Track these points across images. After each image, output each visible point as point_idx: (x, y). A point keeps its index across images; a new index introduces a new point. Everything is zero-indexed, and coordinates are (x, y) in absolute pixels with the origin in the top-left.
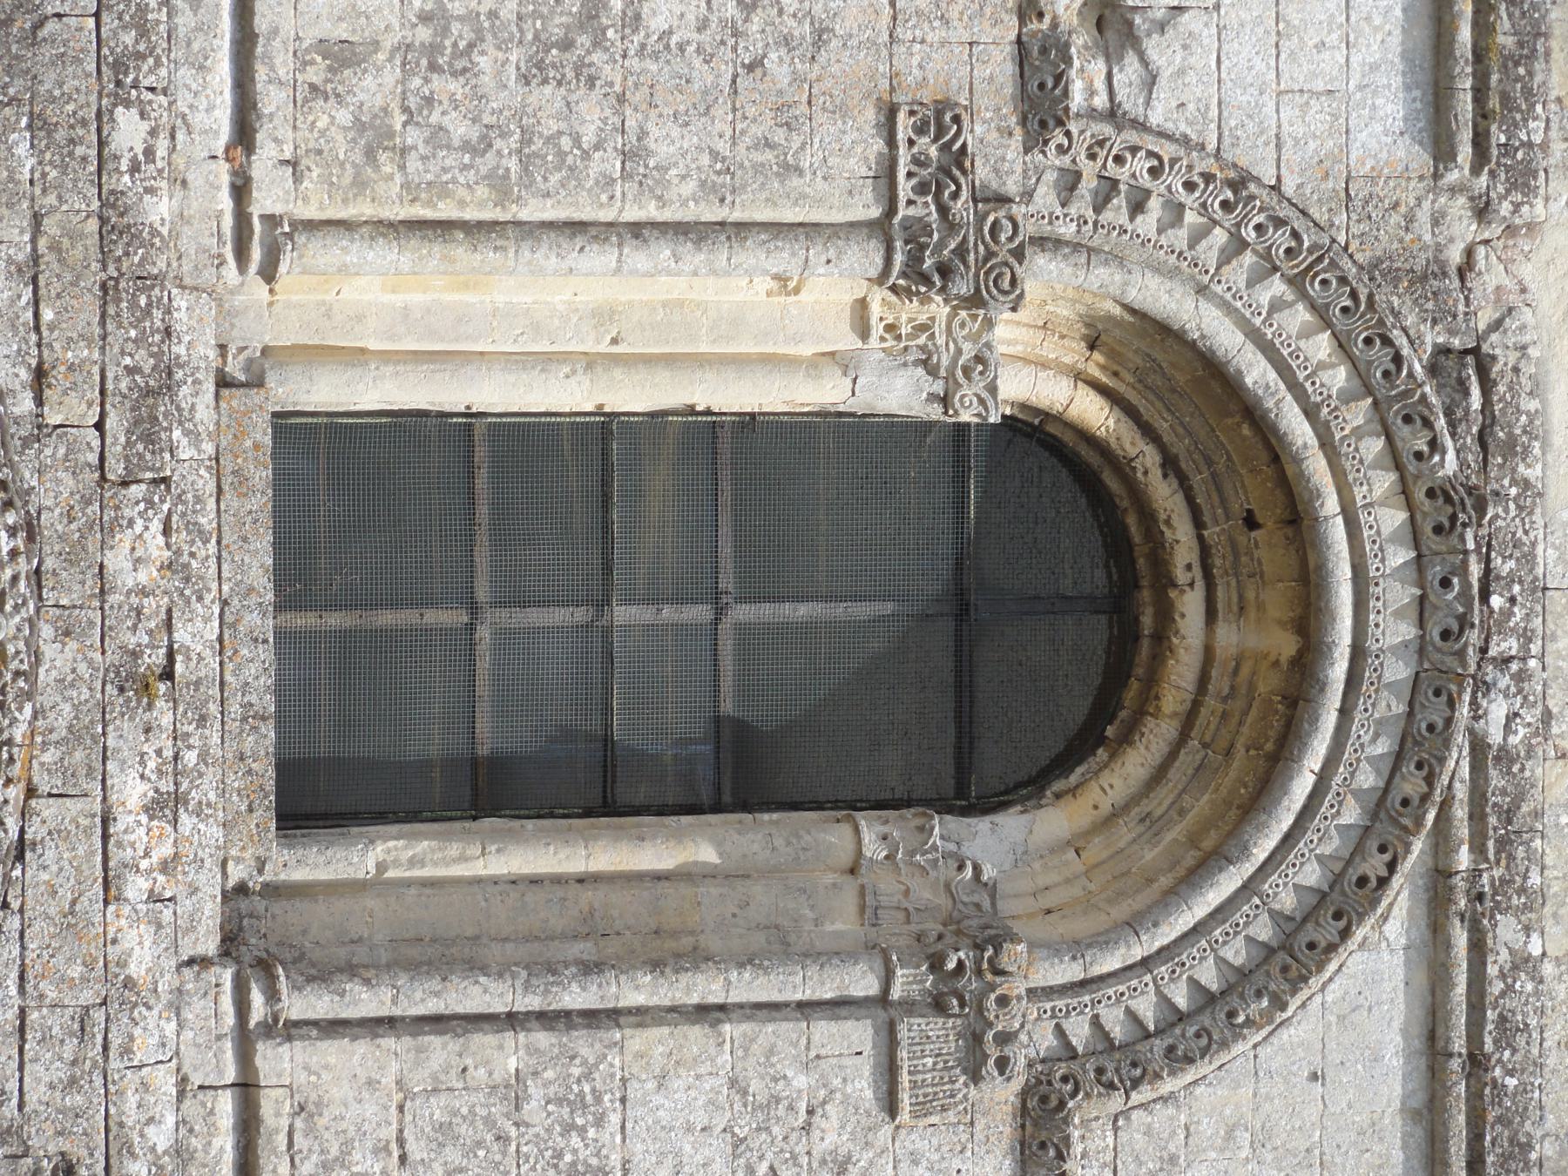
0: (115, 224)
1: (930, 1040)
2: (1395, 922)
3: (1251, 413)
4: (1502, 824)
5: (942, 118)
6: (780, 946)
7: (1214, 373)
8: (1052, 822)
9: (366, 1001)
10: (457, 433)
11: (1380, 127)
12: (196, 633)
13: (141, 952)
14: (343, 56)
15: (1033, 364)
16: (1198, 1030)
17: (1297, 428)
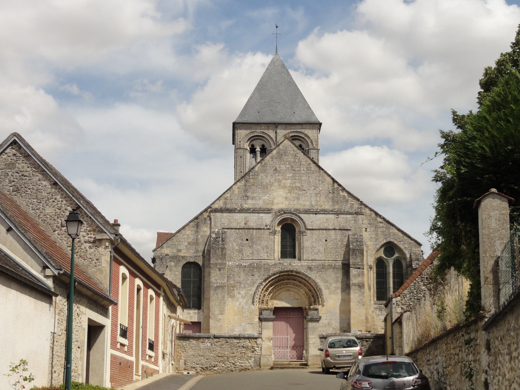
0: (274, 265)
1: (304, 234)
2: (300, 215)
3: (281, 220)
4: (297, 210)
5: (270, 233)
6: (300, 239)
7: (280, 222)
10: (281, 251)
11: (270, 215)
12: (288, 262)
13: (300, 264)
15: (279, 229)
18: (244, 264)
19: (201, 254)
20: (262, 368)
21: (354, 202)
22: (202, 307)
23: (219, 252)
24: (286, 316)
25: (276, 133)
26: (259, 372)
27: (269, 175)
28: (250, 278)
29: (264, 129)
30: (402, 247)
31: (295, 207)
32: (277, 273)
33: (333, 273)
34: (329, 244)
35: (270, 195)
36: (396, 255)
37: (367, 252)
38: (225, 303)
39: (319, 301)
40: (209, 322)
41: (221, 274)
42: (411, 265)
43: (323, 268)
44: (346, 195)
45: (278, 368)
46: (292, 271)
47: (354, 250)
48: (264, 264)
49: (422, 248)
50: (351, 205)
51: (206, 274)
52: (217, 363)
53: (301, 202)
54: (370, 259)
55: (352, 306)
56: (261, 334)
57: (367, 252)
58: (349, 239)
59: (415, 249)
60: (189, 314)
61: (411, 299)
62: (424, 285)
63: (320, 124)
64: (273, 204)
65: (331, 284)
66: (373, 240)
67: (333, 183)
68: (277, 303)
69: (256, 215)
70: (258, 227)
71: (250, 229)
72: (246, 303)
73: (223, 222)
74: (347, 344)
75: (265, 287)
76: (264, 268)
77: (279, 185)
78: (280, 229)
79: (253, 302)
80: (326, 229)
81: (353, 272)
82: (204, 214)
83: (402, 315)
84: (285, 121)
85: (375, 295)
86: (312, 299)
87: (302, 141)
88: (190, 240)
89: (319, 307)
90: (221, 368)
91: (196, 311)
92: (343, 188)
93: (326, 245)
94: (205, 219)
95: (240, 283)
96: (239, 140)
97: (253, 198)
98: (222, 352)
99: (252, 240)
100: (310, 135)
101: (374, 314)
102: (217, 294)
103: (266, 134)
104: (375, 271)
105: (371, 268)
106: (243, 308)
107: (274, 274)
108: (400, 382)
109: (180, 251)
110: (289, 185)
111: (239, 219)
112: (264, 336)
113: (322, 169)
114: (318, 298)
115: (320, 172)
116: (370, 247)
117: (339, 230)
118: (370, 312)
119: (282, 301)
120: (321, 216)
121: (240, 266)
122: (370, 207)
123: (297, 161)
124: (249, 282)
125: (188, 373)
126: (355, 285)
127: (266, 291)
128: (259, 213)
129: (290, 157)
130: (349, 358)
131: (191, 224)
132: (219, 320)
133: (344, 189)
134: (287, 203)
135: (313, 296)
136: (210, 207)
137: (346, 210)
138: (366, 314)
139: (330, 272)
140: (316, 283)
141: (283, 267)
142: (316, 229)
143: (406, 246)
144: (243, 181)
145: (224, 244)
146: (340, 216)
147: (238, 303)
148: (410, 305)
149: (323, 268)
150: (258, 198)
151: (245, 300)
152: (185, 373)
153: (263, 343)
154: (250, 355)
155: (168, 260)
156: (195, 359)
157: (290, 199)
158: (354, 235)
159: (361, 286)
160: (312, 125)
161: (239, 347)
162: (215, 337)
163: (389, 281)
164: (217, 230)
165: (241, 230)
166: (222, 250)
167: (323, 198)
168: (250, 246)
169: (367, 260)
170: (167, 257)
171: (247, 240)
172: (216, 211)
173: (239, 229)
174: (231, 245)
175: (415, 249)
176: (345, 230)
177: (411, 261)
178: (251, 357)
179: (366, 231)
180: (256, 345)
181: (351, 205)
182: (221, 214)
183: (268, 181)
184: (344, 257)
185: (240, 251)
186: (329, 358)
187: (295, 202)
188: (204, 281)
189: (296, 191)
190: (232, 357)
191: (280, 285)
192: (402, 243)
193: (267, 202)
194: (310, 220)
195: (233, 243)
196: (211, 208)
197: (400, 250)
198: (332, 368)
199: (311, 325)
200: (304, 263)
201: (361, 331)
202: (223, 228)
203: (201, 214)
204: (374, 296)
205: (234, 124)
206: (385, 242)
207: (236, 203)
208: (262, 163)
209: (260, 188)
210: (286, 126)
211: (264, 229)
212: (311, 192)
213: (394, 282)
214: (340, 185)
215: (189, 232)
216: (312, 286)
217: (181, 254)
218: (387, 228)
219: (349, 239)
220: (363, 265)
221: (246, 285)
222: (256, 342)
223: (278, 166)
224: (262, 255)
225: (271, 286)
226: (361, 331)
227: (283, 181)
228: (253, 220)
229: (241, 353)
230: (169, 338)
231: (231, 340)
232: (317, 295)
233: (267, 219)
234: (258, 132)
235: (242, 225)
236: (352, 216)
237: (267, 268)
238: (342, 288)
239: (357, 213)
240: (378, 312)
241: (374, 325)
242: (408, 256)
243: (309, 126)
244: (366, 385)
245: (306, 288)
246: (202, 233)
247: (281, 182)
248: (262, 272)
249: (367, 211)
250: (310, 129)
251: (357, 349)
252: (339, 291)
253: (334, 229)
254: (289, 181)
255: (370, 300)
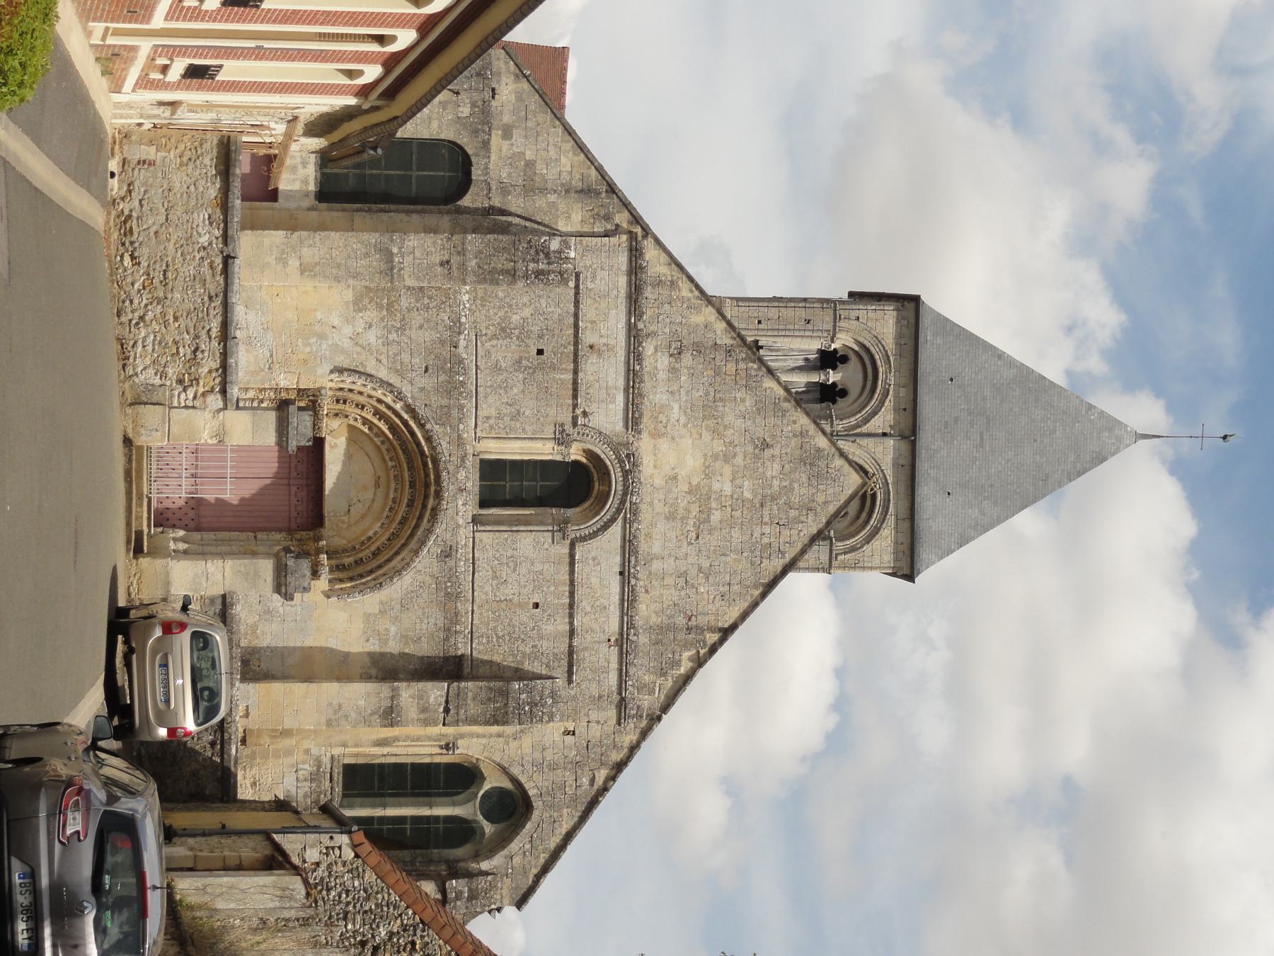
0: (459, 437)
1: (558, 535)
2: (620, 521)
3: (602, 460)
4: (635, 512)
6: (542, 523)
7: (598, 457)
8: (578, 509)
9: (488, 528)
11: (620, 426)
12: (469, 485)
13: (461, 522)
14: (488, 418)
15: (575, 453)
16: (594, 535)
17: (608, 463)
18: (462, 343)
19: (497, 202)
20: (129, 411)
21: (660, 696)
22: (324, 205)
23: (501, 262)
24: (294, 474)
25: (884, 434)
26: (116, 400)
27: (749, 423)
28: (416, 360)
29: (896, 397)
30: (514, 846)
31: (643, 507)
32: (434, 448)
33: (431, 626)
34: (524, 616)
35: (685, 426)
36: (488, 828)
37: (499, 736)
38: (337, 279)
39: (341, 581)
40: (276, 228)
41: (431, 267)
42: (455, 874)
43: (449, 595)
44: (682, 670)
45: (130, 461)
46: (438, 495)
47: (505, 694)
48: (461, 408)
49: (510, 910)
50: (648, 682)
51: (432, 220)
52: (144, 264)
53: (661, 526)
54: (477, 744)
55: (325, 685)
56: (238, 408)
57: (499, 736)
58: (540, 677)
59: (505, 888)
60: (304, 164)
61: (347, 892)
62: (391, 935)
63: (910, 577)
64: (656, 435)
65: (396, 620)
66: (538, 755)
67: (720, 630)
68: (336, 445)
69: (621, 382)
70: (582, 389)
71: (575, 361)
72: (336, 348)
73: (600, 274)
74: (203, 689)
75: (389, 407)
76: (448, 407)
77: (715, 457)
78: (573, 458)
79: (340, 370)
80: (571, 606)
81: (436, 692)
82: (626, 214)
83: (296, 870)
84: (923, 466)
85: (361, 761)
86: (348, 560)
87: (858, 517)
88: (541, 168)
89: (323, 583)
90: (129, 280)
91: (312, 187)
92: (705, 661)
93: (520, 605)
94: (607, 218)
95: (402, 329)
96: (862, 314)
97: (673, 370)
98: (179, 284)
99: (541, 367)
100: (876, 543)
101: (302, 757)
102: (367, 255)
103: (882, 403)
104: (437, 760)
105: (447, 747)
106: (322, 336)
107: (429, 439)
108: (82, 930)
109: (507, 134)
110: (716, 486)
111: (607, 324)
112: (231, 414)
113: (764, 595)
114: (351, 579)
115: (756, 588)
116: (514, 744)
117: (570, 646)
118: (306, 744)
119: (344, 463)
120: (616, 589)
121: (456, 327)
122: (644, 745)
123: (793, 513)
124: (406, 357)
125: (113, 175)
126: (392, 698)
127: (377, 413)
128: (626, 390)
129: (803, 491)
130: (160, 697)
131: (593, 172)
132: (282, 261)
133: (700, 662)
134: (658, 482)
135: (359, 562)
136: (647, 231)
137: (632, 671)
138: (299, 731)
139: (436, 618)
140: (399, 572)
141: (451, 468)
142: (572, 572)
143: (517, 860)
144: (729, 342)
145: (526, 277)
146: (615, 650)
147: (336, 323)
148: (328, 890)
149: (449, 595)
150: (675, 388)
151: (347, 344)
152: (113, 165)
153: (208, 415)
154: (170, 371)
155: (476, 96)
156: (156, 195)
157: (670, 491)
158: (553, 694)
159: (390, 716)
160: (908, 553)
161: (197, 337)
162: (228, 260)
163: (406, 805)
164: (572, 255)
165: (571, 331)
166: (508, 272)
167: (671, 595)
168: (520, 362)
169: (472, 735)
170: (487, 94)
171: (540, 352)
172: (635, 252)
173: (576, 326)
174: (525, 300)
175: (505, 888)
176: (570, 665)
177: (470, 875)
178: (163, 375)
179: (567, 733)
180: (201, 390)
181: (648, 682)
182: (624, 268)
183: (729, 419)
184: (484, 662)
185: (503, 330)
186: (158, 632)
187: (659, 507)
188: (408, 212)
189: (695, 509)
190: (164, 314)
191: (395, 458)
192: (528, 846)
193: (662, 417)
194: (603, 552)
195: (533, 306)
196: (645, 236)
197: (502, 841)
198: (127, 642)
199: (266, 567)
200: (464, 534)
201: (247, 715)
202: (577, 275)
203: (626, 205)
204: (357, 755)
205: (916, 300)
206: (531, 793)
207: (661, 318)
208: (786, 400)
209: (707, 394)
210: (908, 468)
211: (575, 406)
212: (691, 560)
213: (402, 820)
214: (713, 650)
215: (566, 164)
216: (389, 560)
217: (496, 139)
218: (575, 799)
219: (540, 677)
220: (457, 723)
221: (394, 349)
222: (212, 390)
223: (777, 451)
224: (491, 400)
225: (393, 428)
226: (247, 715)
227: (727, 470)
228: (605, 374)
229: (176, 342)
230: (228, 120)
231: (219, 310)
232: (361, 576)
233: (607, 416)
234: (889, 377)
235: (588, 338)
236: (614, 688)
237: (448, 414)
238: (382, 655)
239: (622, 704)
240: (307, 768)
241: (265, 756)
242: (485, 865)
243: (907, 540)
244: (74, 823)
245: (383, 539)
246: (562, 206)
247: (726, 461)
248: (437, 401)
249: (629, 738)
250: (896, 543)
251: (190, 724)
252: (374, 646)
253: (572, 633)
254: (728, 489)
255: (345, 745)
